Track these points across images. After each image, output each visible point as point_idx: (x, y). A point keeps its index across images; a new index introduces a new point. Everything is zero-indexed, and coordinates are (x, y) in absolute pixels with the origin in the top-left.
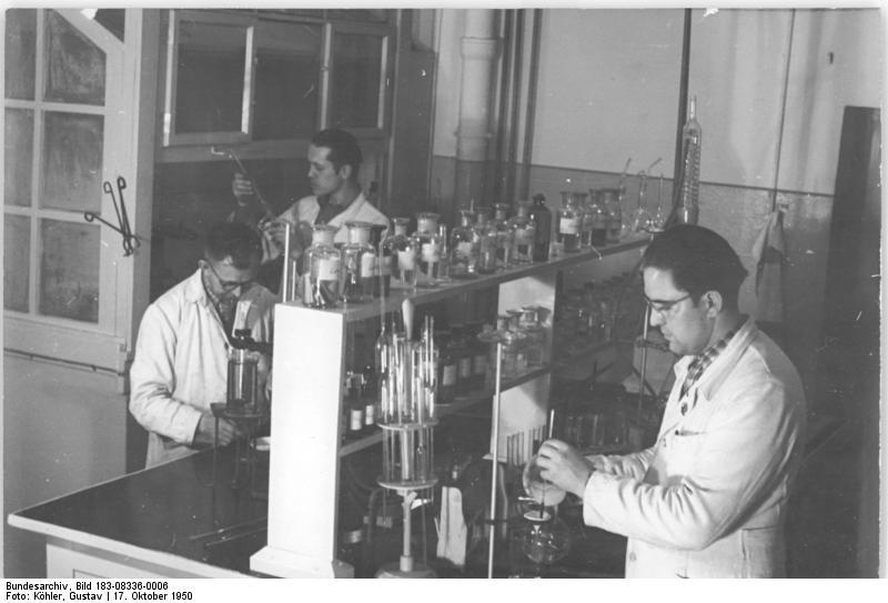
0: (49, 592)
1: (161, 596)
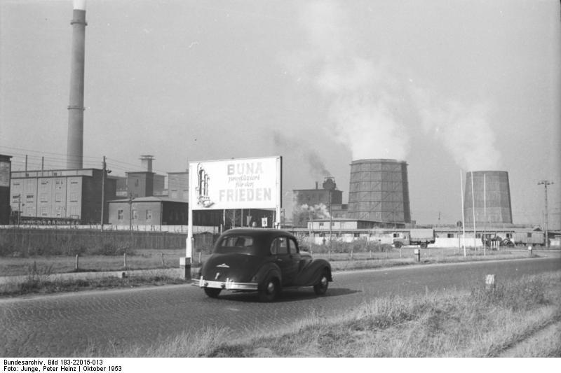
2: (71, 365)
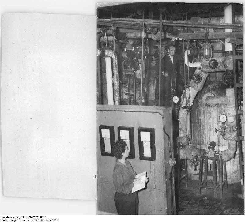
2: (32, 219)
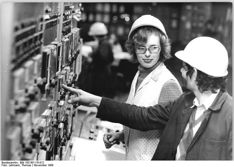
0: (13, 164)
1: (45, 165)
2: (30, 164)
